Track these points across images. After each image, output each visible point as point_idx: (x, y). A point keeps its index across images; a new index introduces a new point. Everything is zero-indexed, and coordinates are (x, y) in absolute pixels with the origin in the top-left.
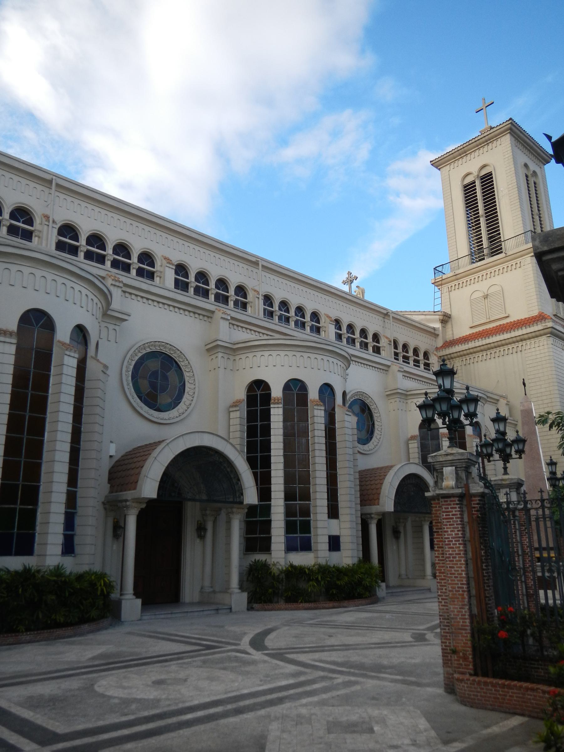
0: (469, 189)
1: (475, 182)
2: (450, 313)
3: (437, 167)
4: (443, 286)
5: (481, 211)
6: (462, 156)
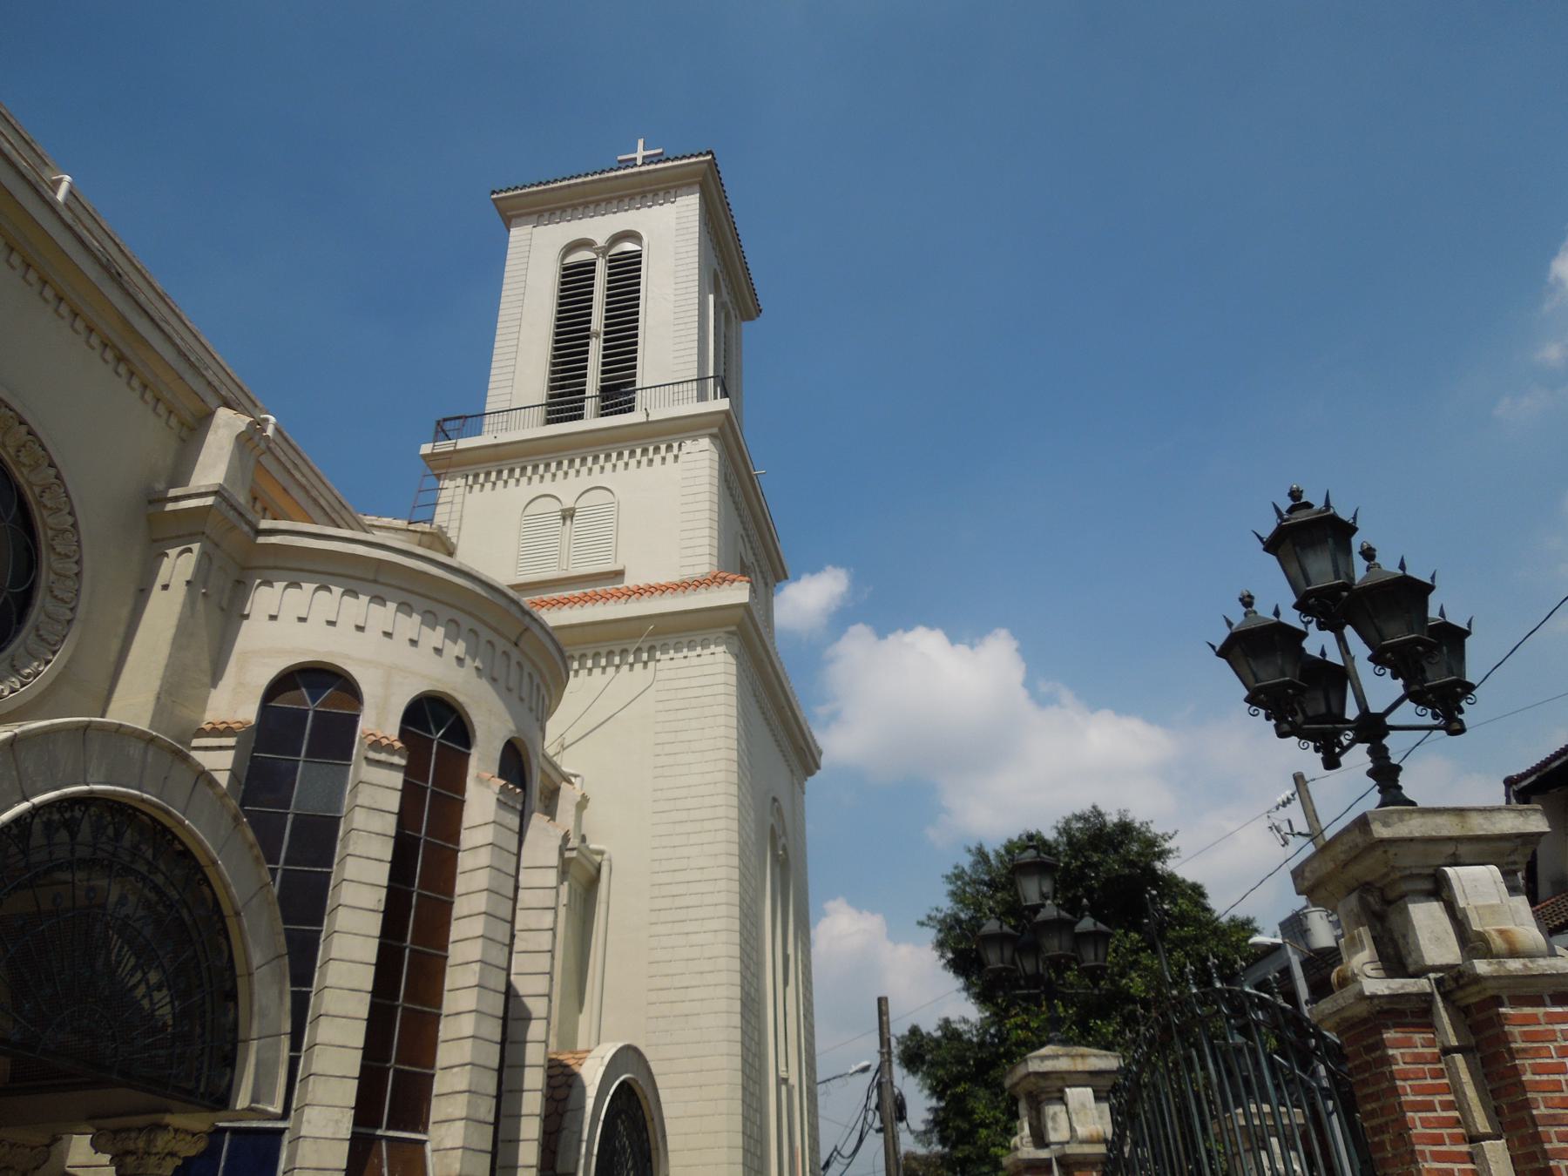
0: (575, 281)
1: (594, 264)
2: (454, 540)
3: (502, 212)
4: (450, 470)
5: (597, 321)
6: (576, 202)
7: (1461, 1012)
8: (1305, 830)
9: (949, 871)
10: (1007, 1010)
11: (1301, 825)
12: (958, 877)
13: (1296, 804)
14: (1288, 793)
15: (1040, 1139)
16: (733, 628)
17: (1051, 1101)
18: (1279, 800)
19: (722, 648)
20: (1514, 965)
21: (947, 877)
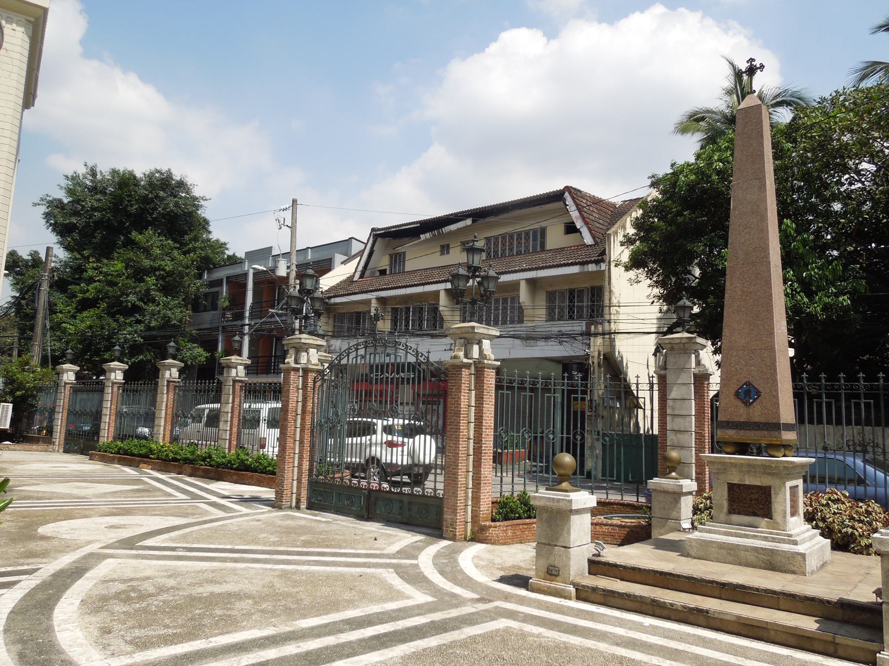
7: (476, 368)
8: (290, 225)
9: (70, 174)
10: (88, 257)
11: (289, 222)
12: (73, 178)
13: (290, 212)
14: (287, 206)
15: (296, 361)
16: (33, 20)
17: (303, 351)
18: (282, 208)
19: (21, 29)
20: (490, 362)
21: (67, 177)
